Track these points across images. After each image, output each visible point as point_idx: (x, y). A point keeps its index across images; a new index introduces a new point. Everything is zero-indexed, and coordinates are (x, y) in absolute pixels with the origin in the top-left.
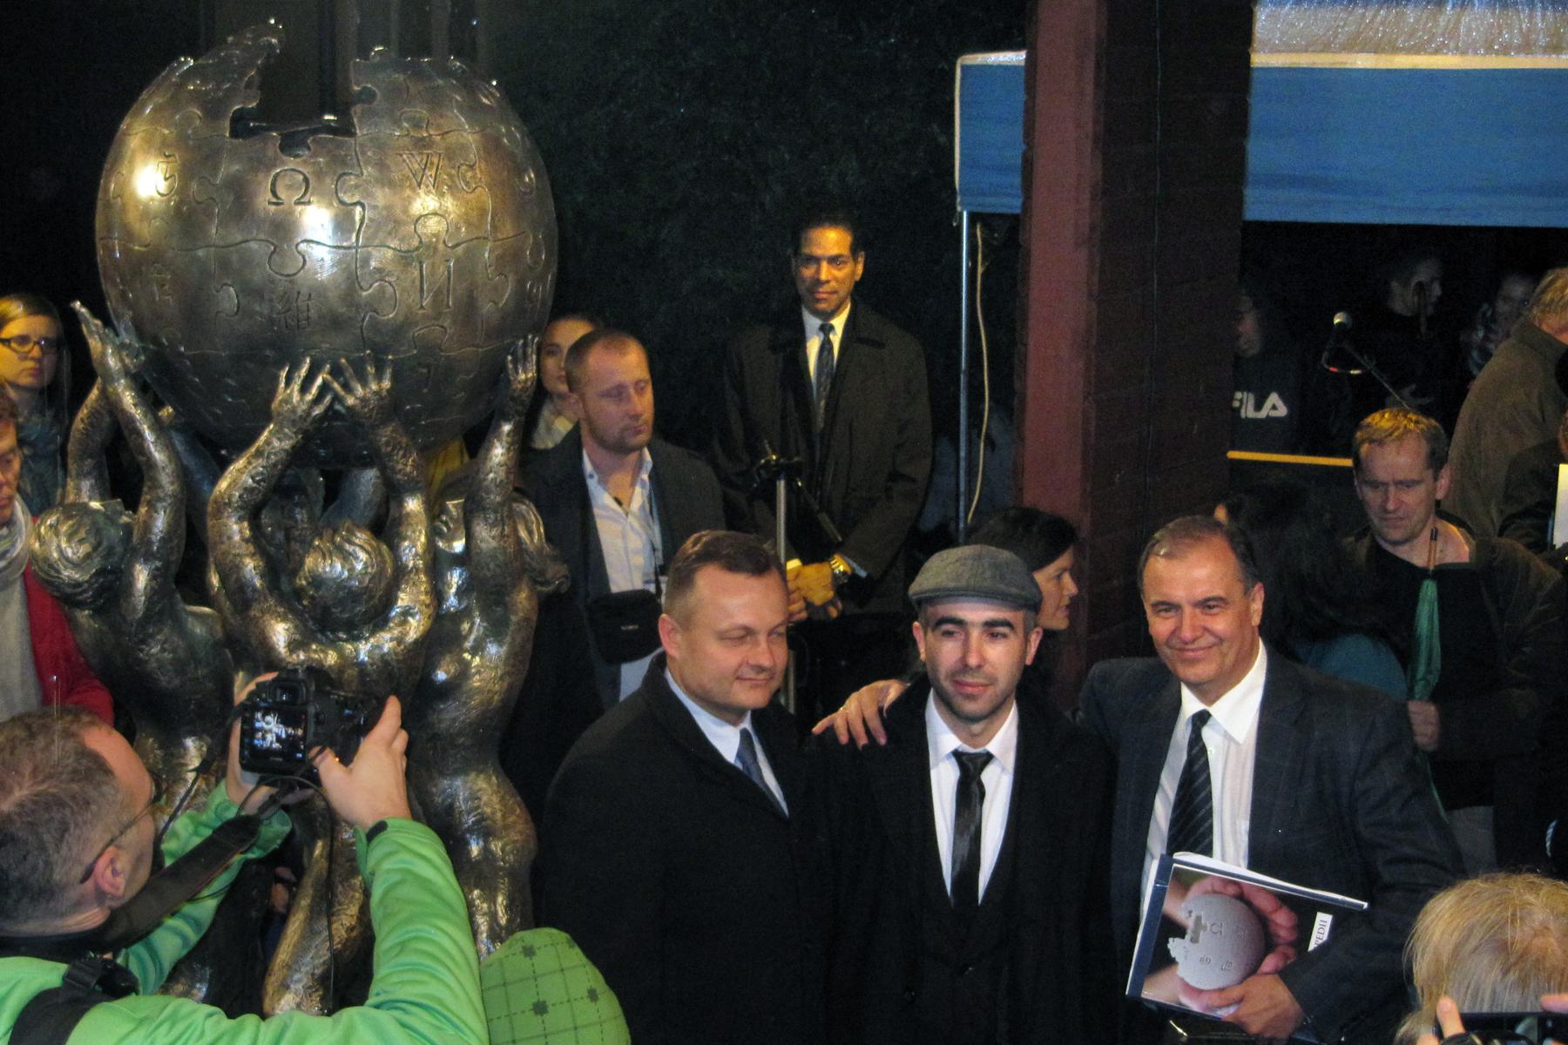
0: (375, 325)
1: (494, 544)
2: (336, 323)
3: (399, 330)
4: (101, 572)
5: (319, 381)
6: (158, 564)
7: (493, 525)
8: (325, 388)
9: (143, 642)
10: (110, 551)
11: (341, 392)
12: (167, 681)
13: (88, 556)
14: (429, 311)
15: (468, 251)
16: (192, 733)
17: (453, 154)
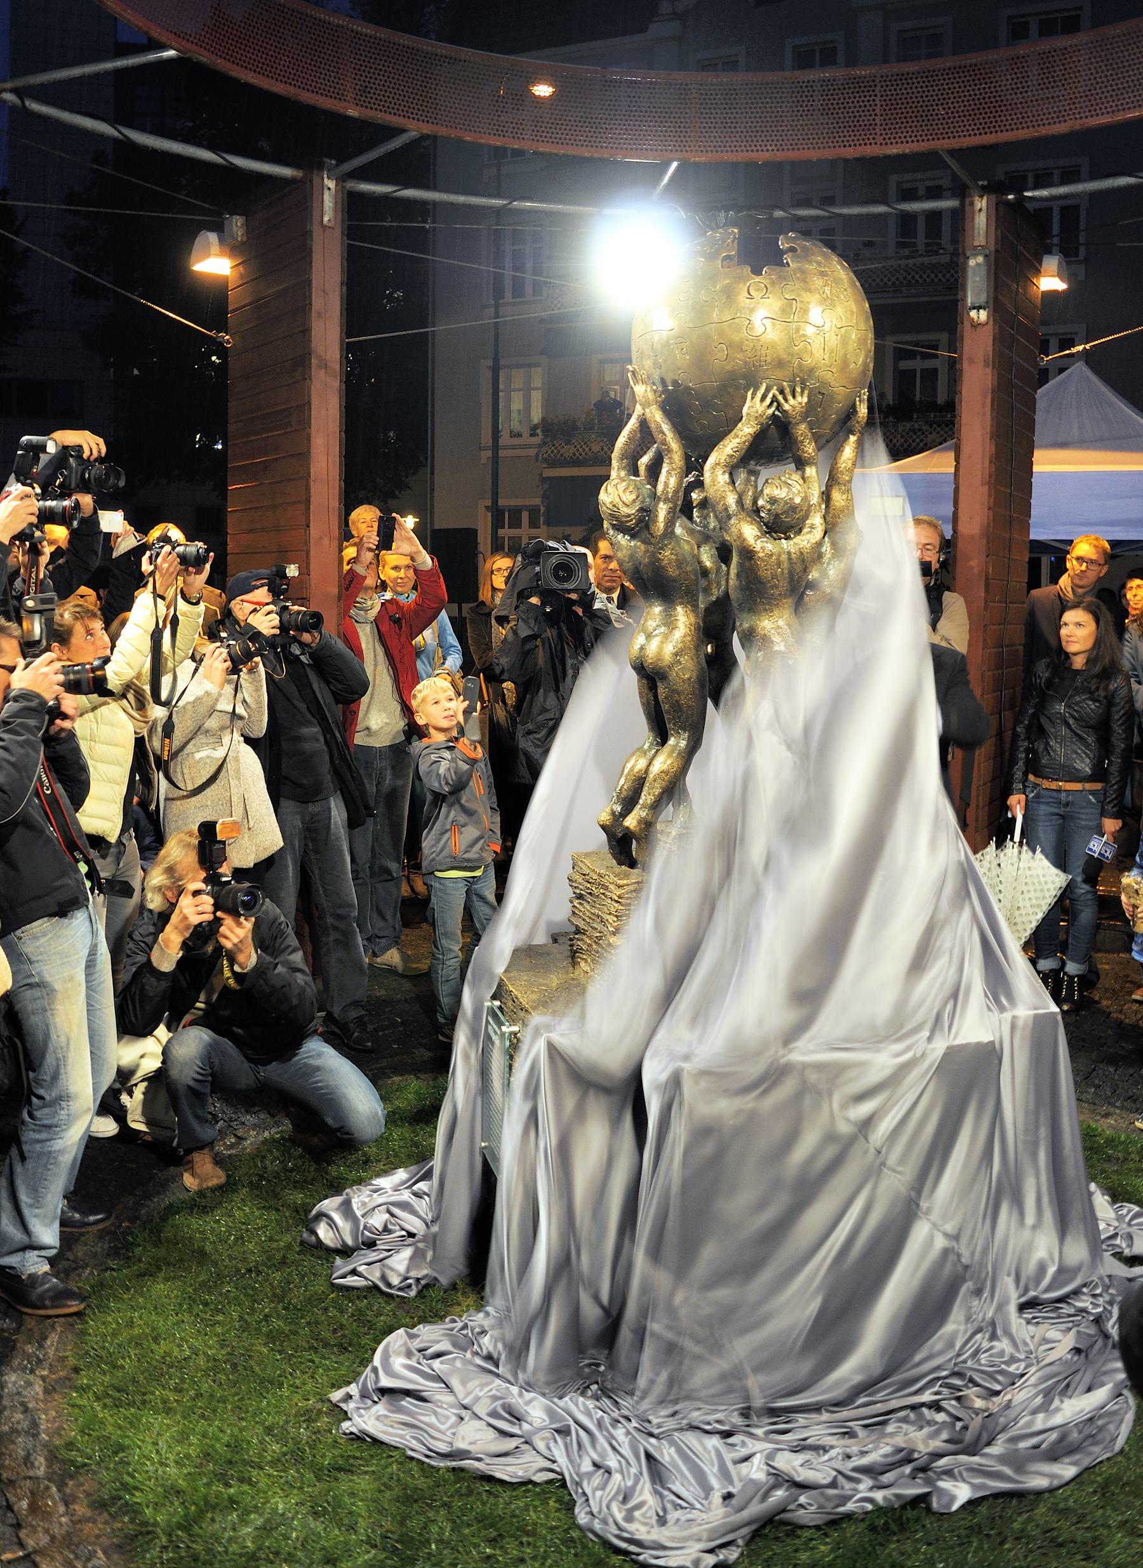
0: (800, 366)
1: (843, 503)
2: (780, 364)
3: (811, 370)
4: (641, 510)
5: (770, 395)
6: (670, 505)
7: (843, 493)
8: (774, 398)
9: (662, 548)
10: (643, 502)
11: (782, 401)
12: (672, 572)
13: (634, 501)
14: (826, 362)
15: (847, 332)
16: (681, 603)
17: (837, 281)
